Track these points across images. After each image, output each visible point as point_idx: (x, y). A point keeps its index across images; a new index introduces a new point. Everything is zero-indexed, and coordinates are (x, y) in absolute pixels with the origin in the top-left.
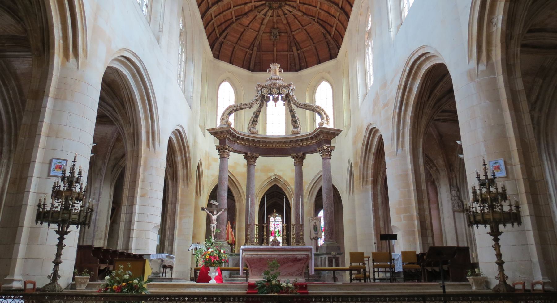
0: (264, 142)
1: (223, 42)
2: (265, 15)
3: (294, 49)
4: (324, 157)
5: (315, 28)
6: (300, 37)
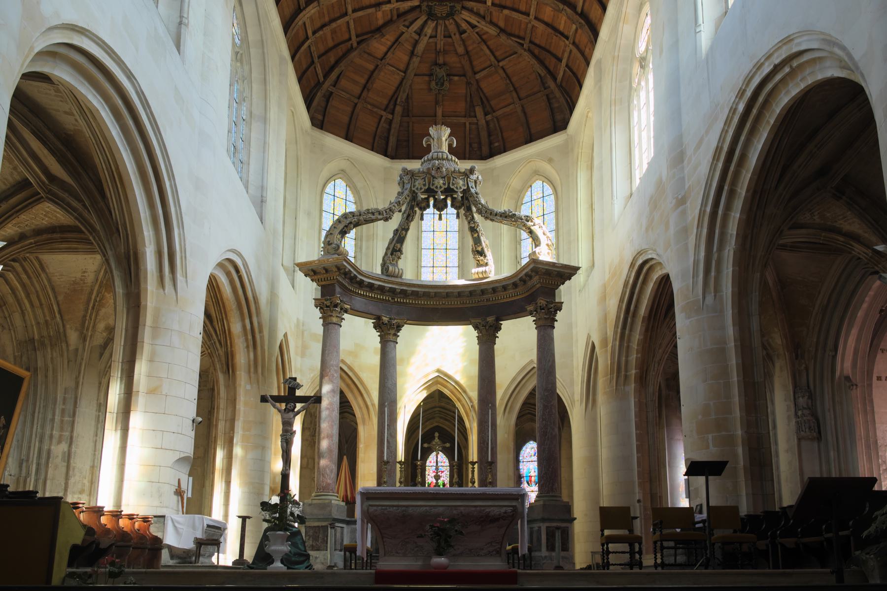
0: (415, 294)
1: (331, 93)
2: (420, 32)
4: (541, 323)
5: (524, 64)
6: (492, 84)
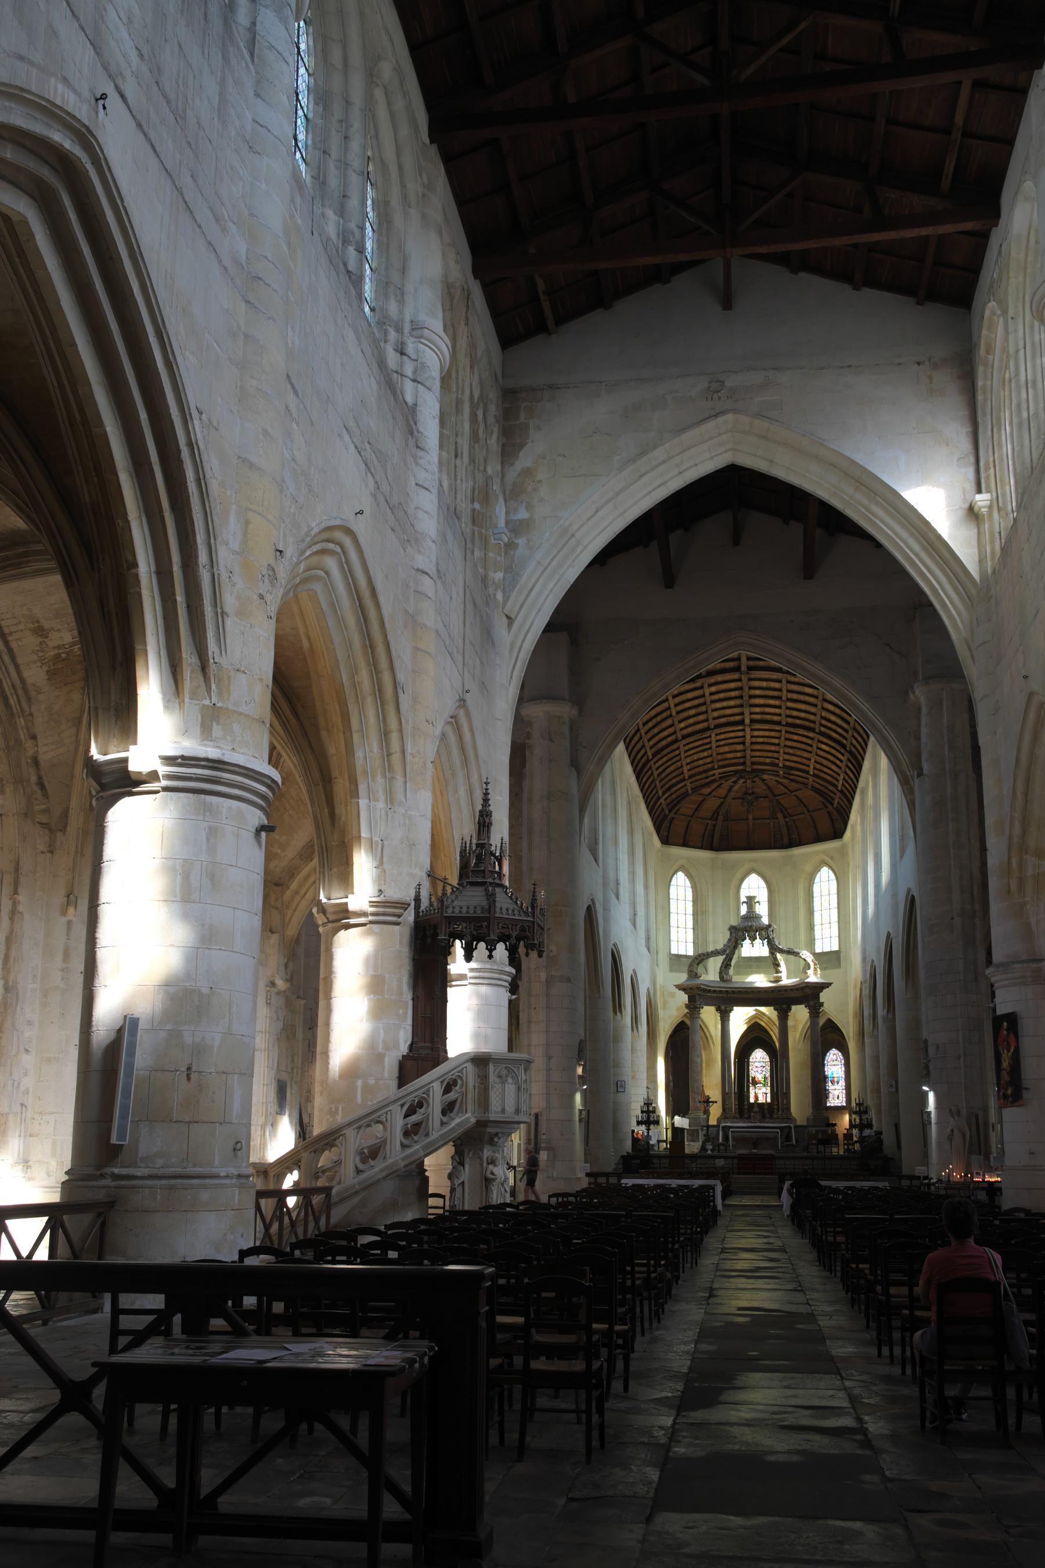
2: (735, 782)
3: (780, 815)
5: (807, 794)
